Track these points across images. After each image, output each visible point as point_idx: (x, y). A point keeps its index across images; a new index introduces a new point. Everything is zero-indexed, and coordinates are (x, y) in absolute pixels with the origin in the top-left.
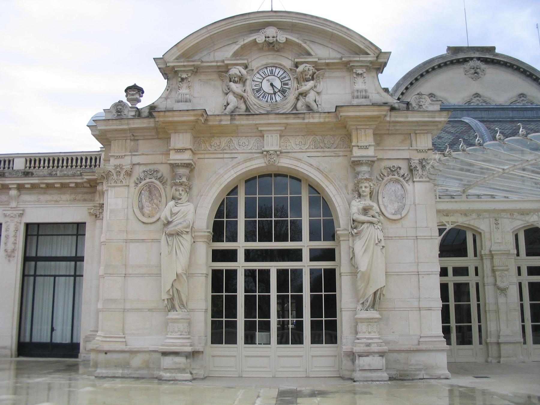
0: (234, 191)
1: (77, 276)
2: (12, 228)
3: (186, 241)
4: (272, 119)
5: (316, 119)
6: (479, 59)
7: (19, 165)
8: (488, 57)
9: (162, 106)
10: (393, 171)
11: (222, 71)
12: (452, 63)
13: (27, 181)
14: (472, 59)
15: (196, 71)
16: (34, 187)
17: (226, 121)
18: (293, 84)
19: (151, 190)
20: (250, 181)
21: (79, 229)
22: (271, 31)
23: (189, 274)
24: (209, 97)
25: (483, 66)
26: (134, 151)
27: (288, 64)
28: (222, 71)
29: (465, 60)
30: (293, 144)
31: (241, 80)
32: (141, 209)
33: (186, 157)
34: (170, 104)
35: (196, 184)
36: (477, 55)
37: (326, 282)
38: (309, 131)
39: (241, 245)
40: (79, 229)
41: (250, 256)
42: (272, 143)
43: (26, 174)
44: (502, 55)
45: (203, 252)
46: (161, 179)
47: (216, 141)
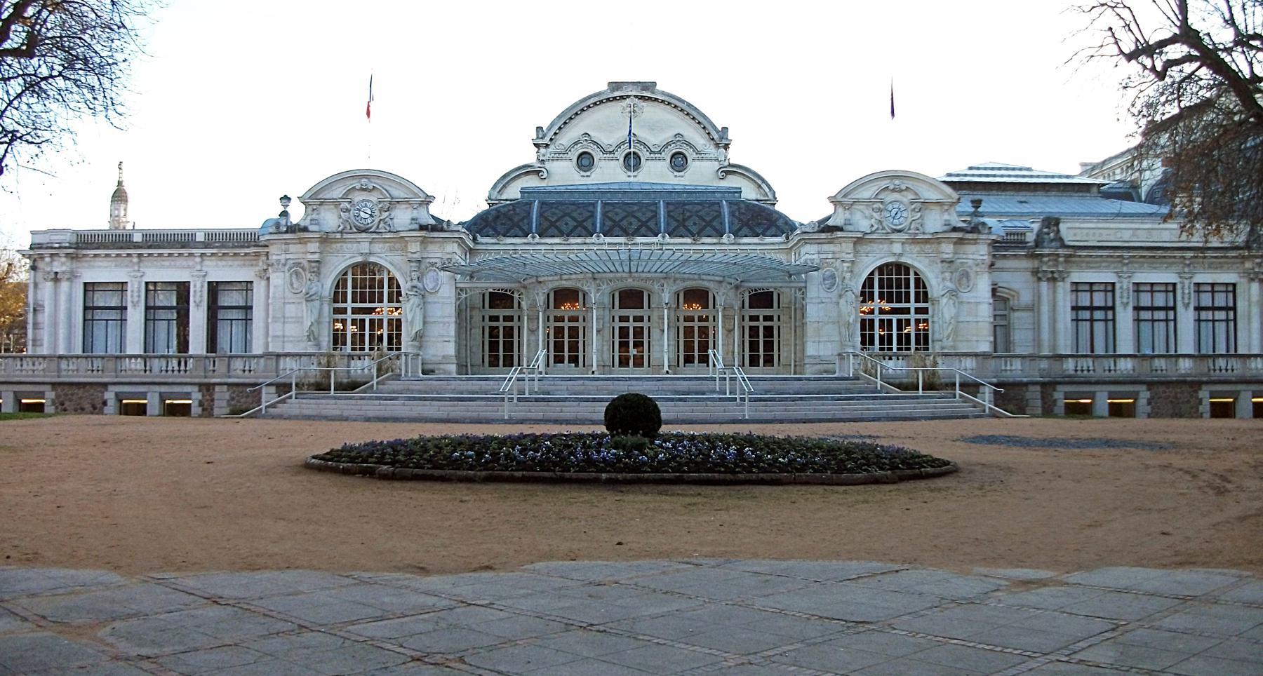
0: (346, 274)
1: (247, 320)
2: (198, 285)
3: (317, 303)
4: (364, 235)
5: (389, 235)
6: (636, 96)
7: (200, 237)
8: (647, 93)
9: (302, 224)
10: (433, 265)
11: (336, 204)
12: (608, 100)
13: (208, 251)
14: (628, 96)
15: (321, 204)
16: (213, 254)
17: (338, 236)
18: (377, 213)
19: (297, 273)
20: (354, 267)
21: (247, 286)
22: (364, 181)
23: (318, 322)
24: (330, 220)
25: (641, 103)
26: (286, 251)
27: (374, 199)
28: (336, 204)
29: (622, 97)
30: (377, 247)
31: (348, 210)
32: (292, 285)
33: (316, 257)
34: (307, 223)
35: (323, 270)
36: (634, 93)
37: (397, 325)
38: (385, 241)
39: (349, 305)
40: (247, 286)
41: (355, 311)
42: (365, 247)
43: (206, 245)
44: (663, 93)
45: (327, 310)
46: (303, 268)
47: (334, 246)
